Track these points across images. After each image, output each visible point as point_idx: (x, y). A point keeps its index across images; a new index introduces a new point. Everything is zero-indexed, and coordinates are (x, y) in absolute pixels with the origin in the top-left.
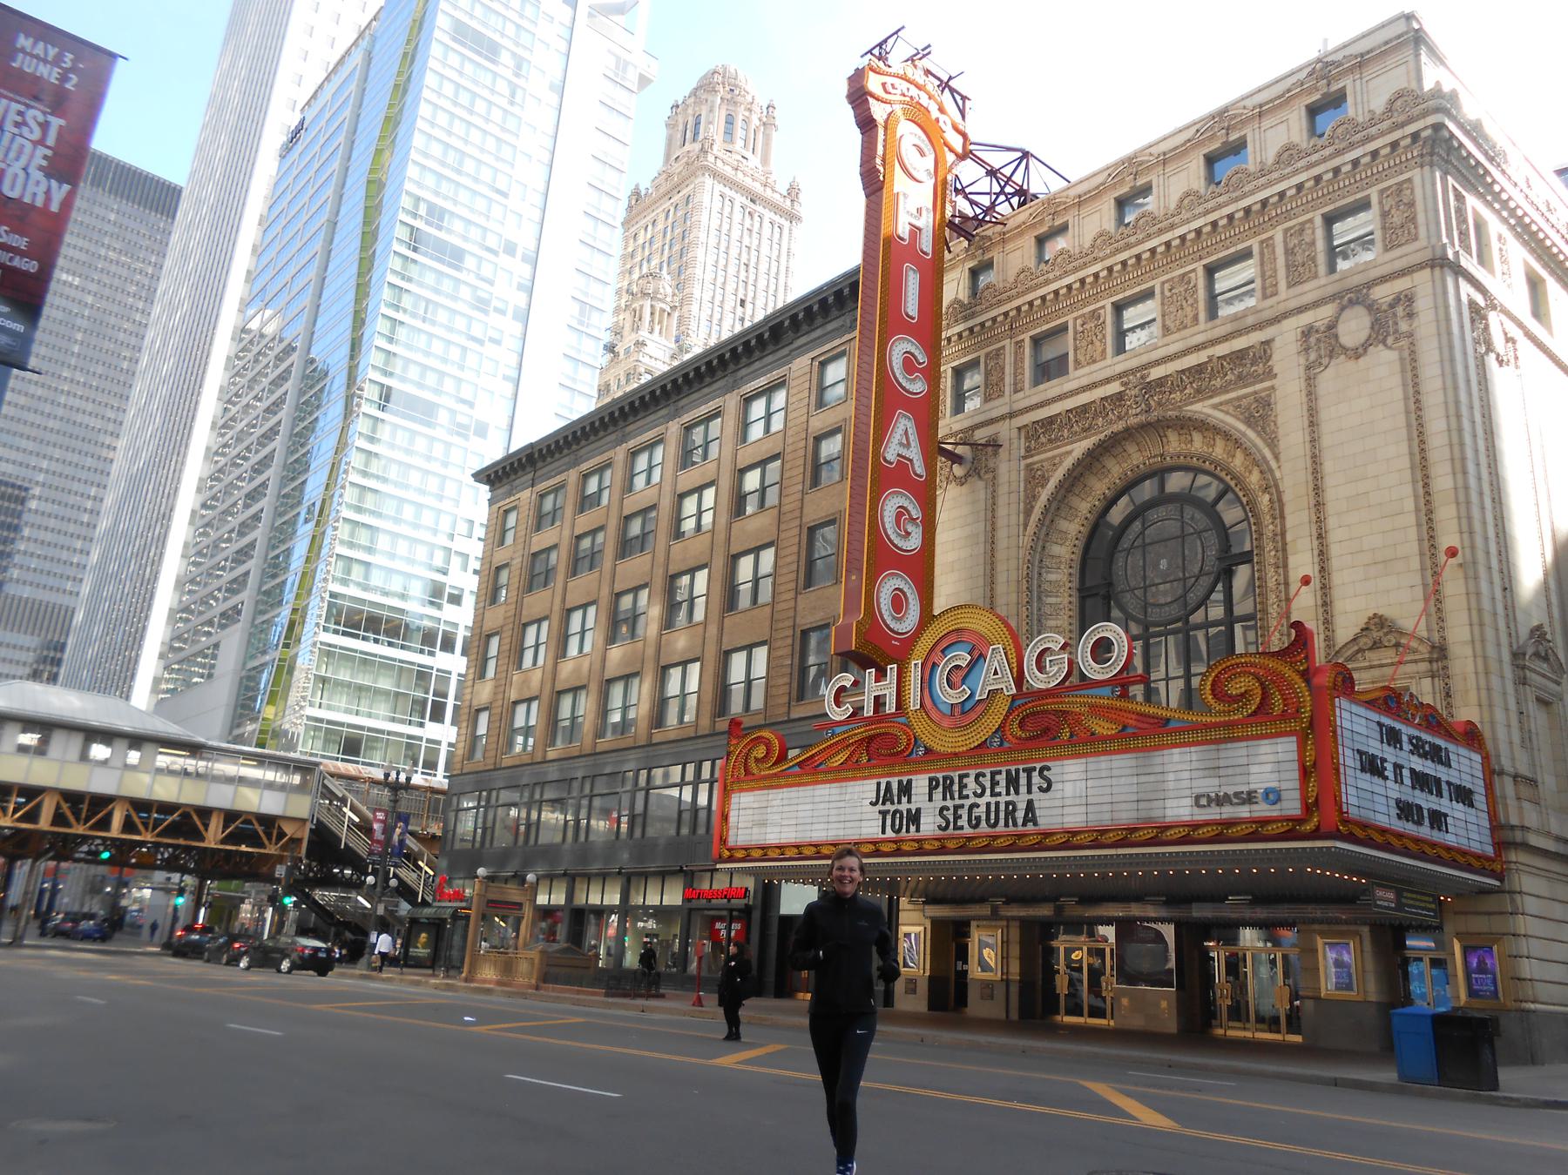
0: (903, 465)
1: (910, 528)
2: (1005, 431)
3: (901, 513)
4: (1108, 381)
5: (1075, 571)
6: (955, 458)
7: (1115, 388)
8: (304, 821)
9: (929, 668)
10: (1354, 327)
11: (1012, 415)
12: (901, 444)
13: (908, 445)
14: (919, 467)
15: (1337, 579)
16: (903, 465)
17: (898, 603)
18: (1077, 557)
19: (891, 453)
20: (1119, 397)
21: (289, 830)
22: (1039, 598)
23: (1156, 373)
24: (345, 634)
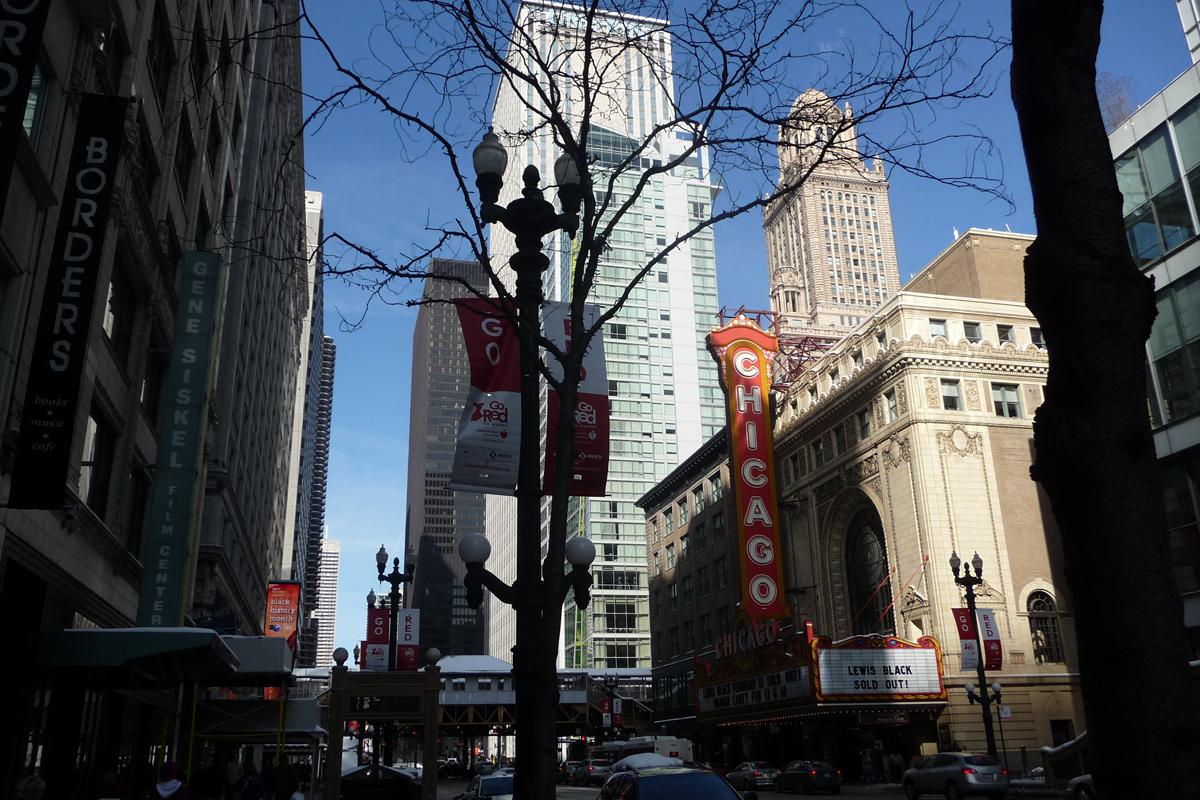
0: (758, 523)
1: (766, 552)
2: (809, 491)
3: (759, 548)
4: (834, 470)
5: (843, 559)
6: (793, 507)
7: (836, 473)
8: (584, 704)
9: (737, 636)
10: (896, 450)
11: (810, 484)
12: (755, 512)
13: (760, 512)
14: (767, 521)
15: (902, 568)
16: (758, 523)
17: (763, 589)
18: (843, 553)
19: (750, 519)
20: (838, 478)
21: (579, 710)
22: (831, 574)
23: (848, 467)
24: (605, 588)
